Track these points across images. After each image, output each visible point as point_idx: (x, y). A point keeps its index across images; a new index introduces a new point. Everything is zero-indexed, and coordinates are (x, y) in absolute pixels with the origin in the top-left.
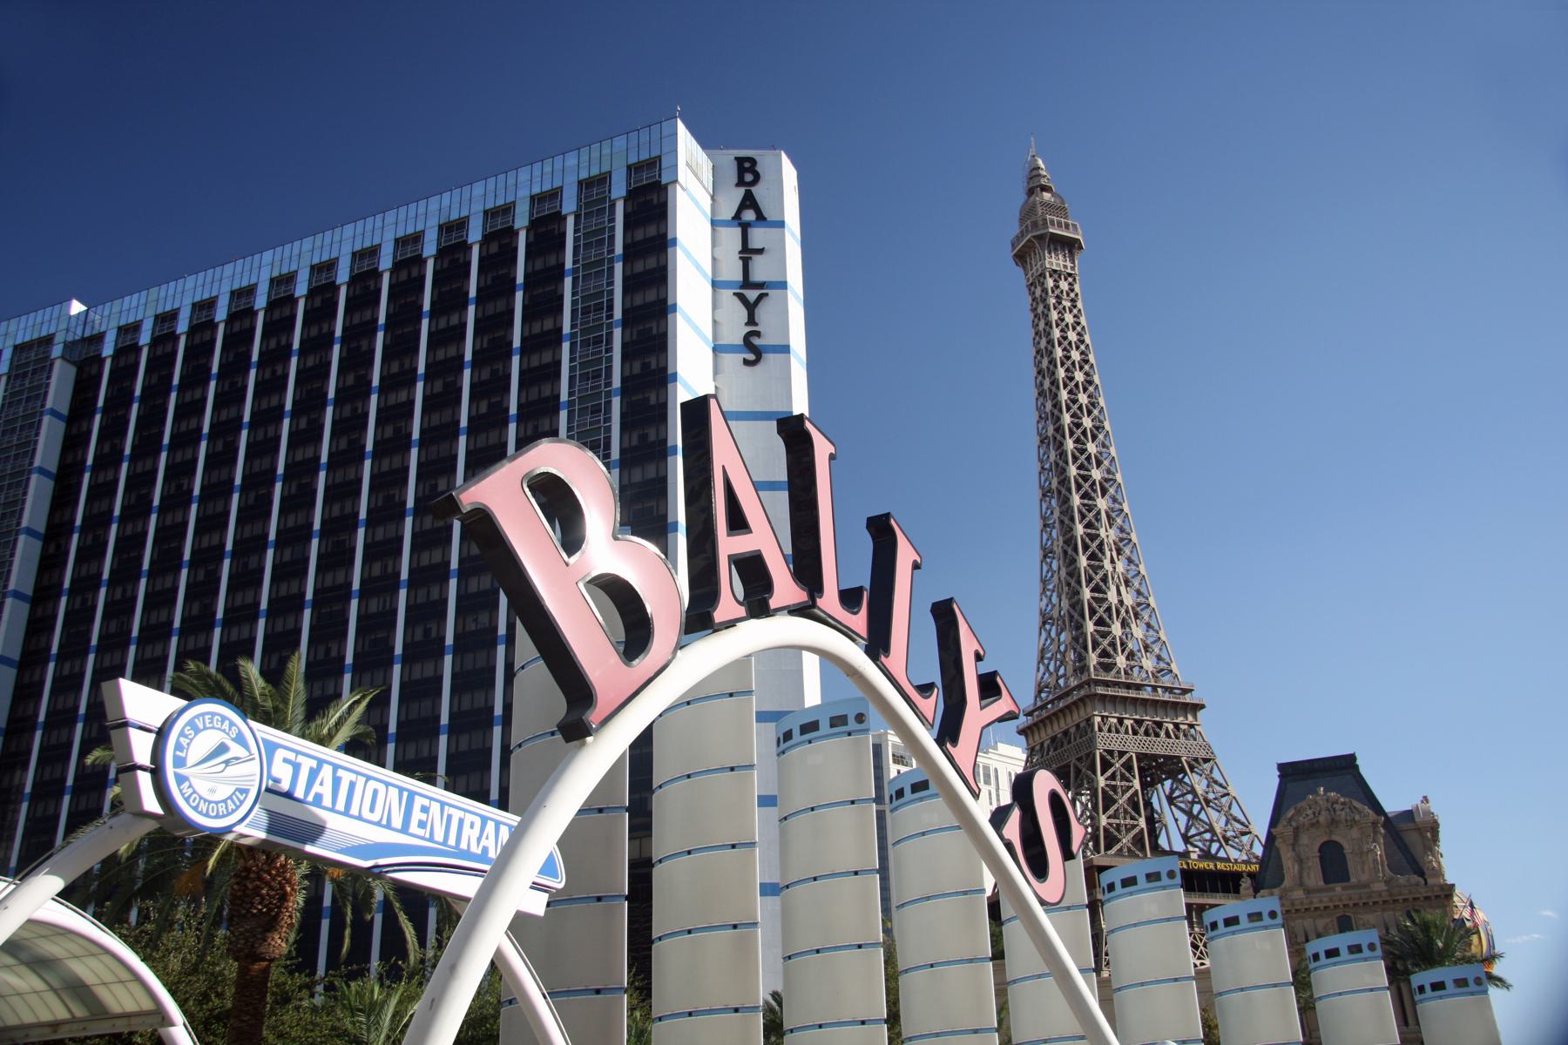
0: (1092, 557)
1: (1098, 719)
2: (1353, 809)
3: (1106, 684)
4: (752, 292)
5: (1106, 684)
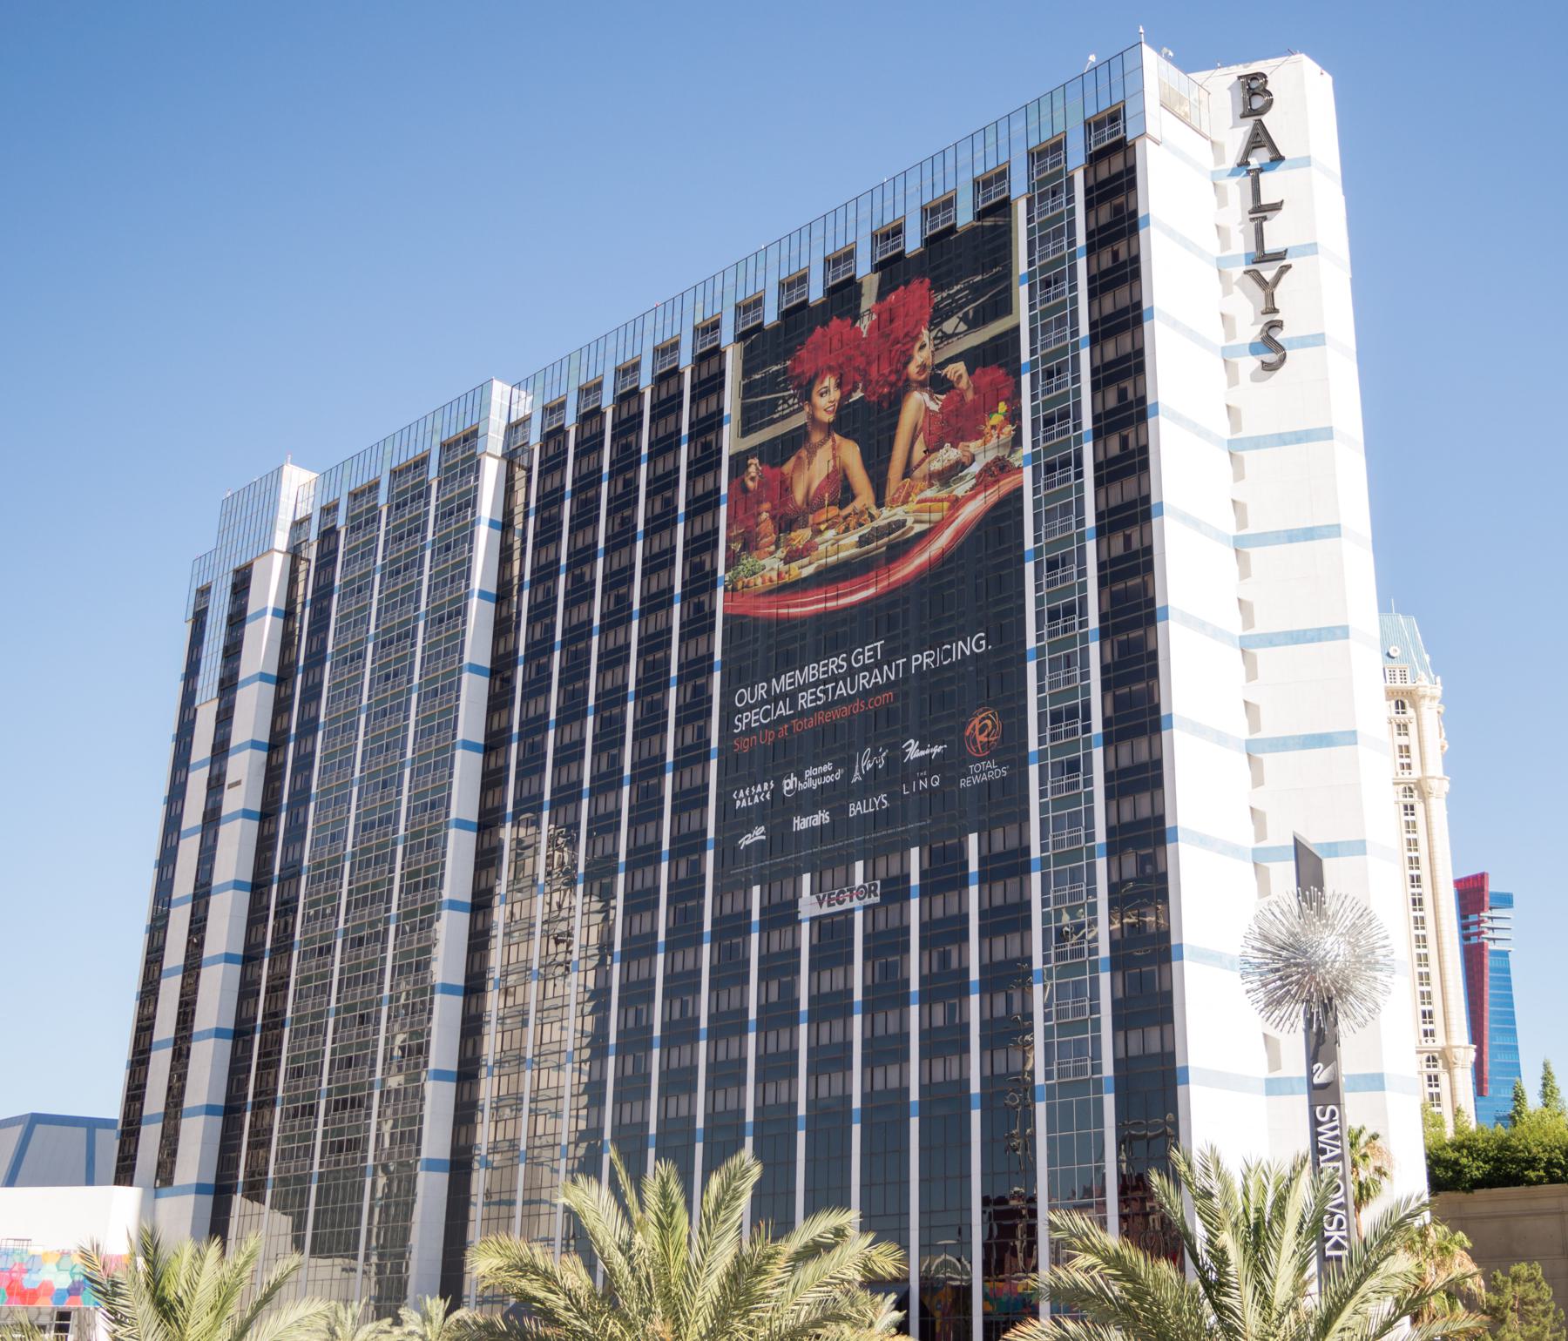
4: (1265, 265)
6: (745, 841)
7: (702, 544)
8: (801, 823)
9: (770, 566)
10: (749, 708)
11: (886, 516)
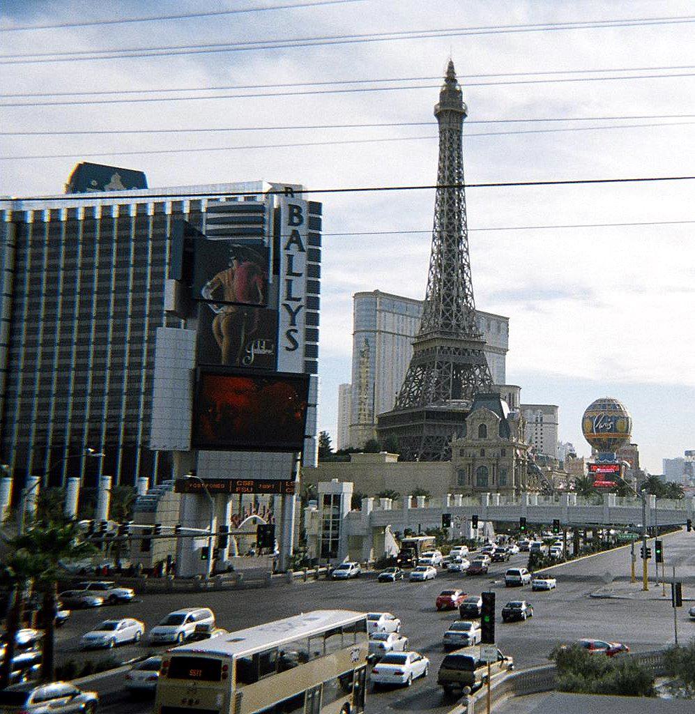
2: (492, 414)
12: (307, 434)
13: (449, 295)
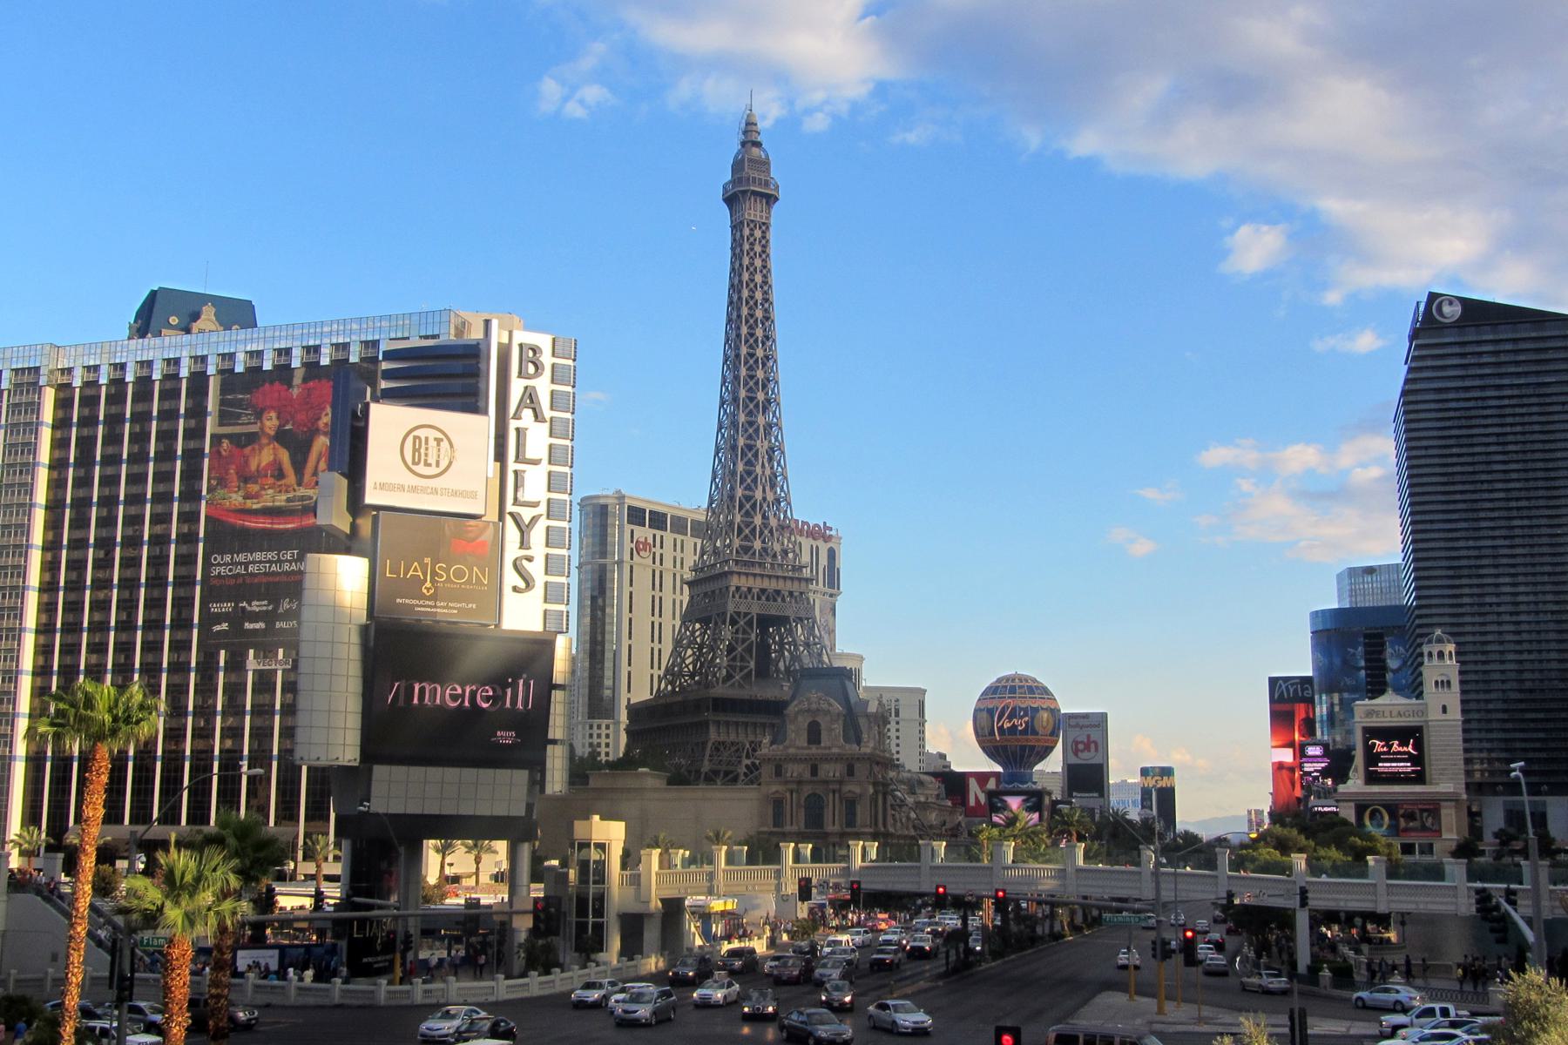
0: (749, 463)
1: (733, 589)
3: (746, 563)
5: (746, 563)
6: (217, 628)
7: (192, 474)
8: (247, 626)
9: (236, 499)
10: (219, 564)
11: (302, 492)
12: (550, 736)
13: (748, 499)
